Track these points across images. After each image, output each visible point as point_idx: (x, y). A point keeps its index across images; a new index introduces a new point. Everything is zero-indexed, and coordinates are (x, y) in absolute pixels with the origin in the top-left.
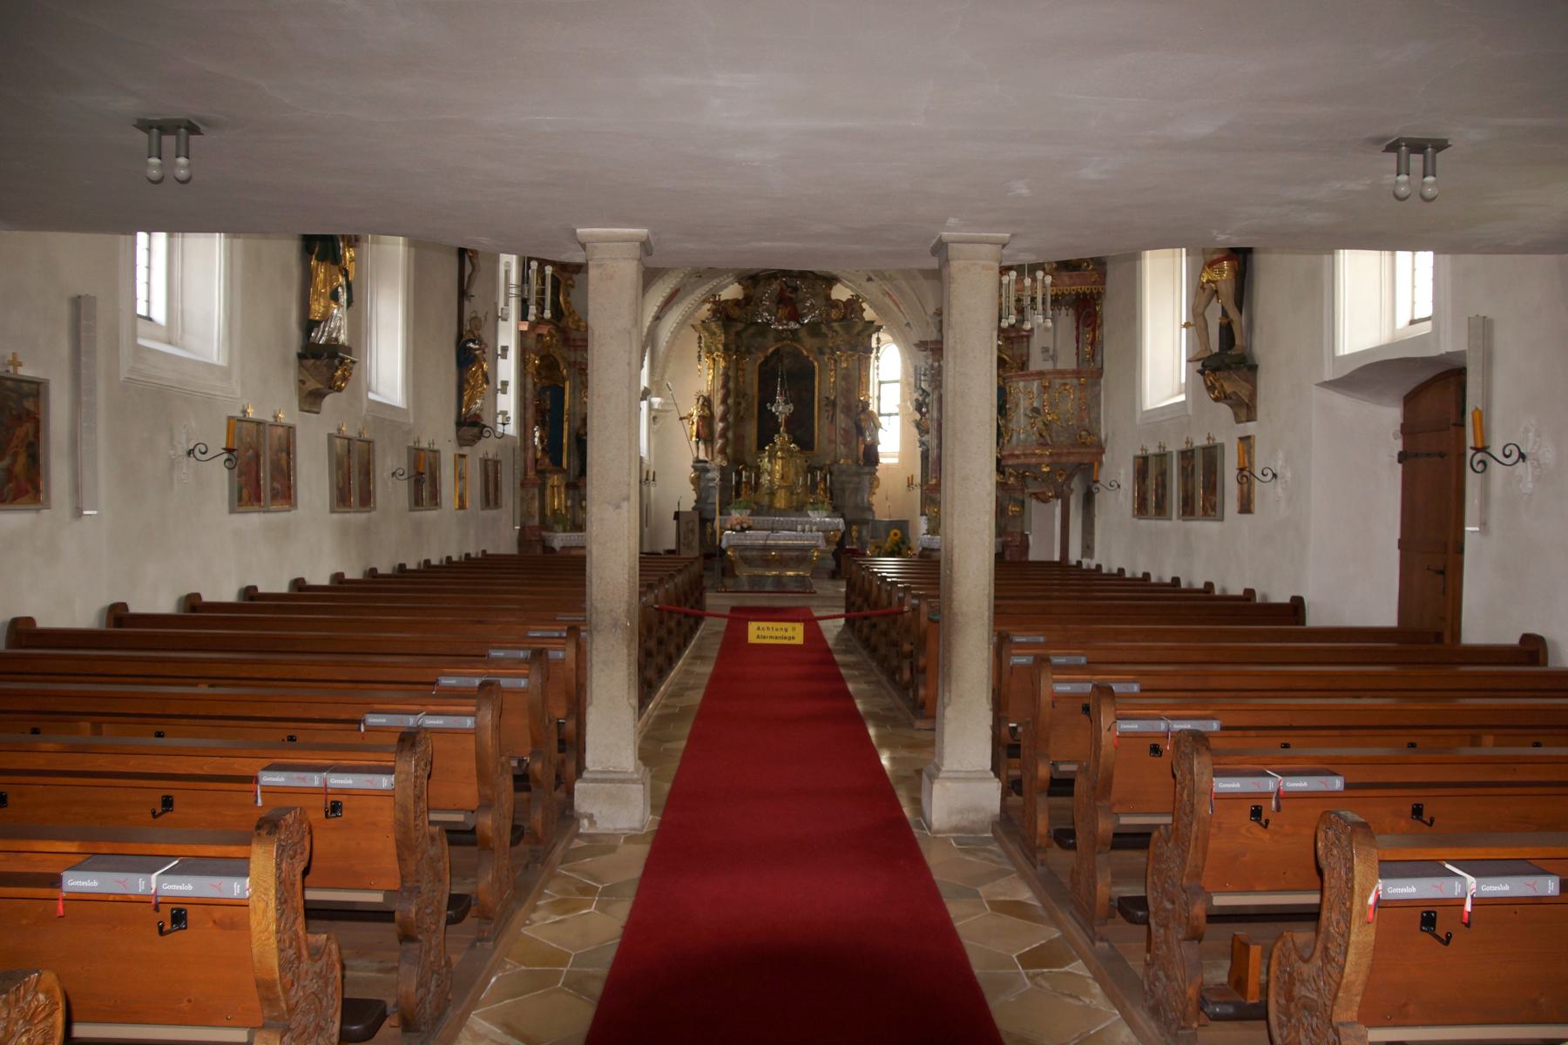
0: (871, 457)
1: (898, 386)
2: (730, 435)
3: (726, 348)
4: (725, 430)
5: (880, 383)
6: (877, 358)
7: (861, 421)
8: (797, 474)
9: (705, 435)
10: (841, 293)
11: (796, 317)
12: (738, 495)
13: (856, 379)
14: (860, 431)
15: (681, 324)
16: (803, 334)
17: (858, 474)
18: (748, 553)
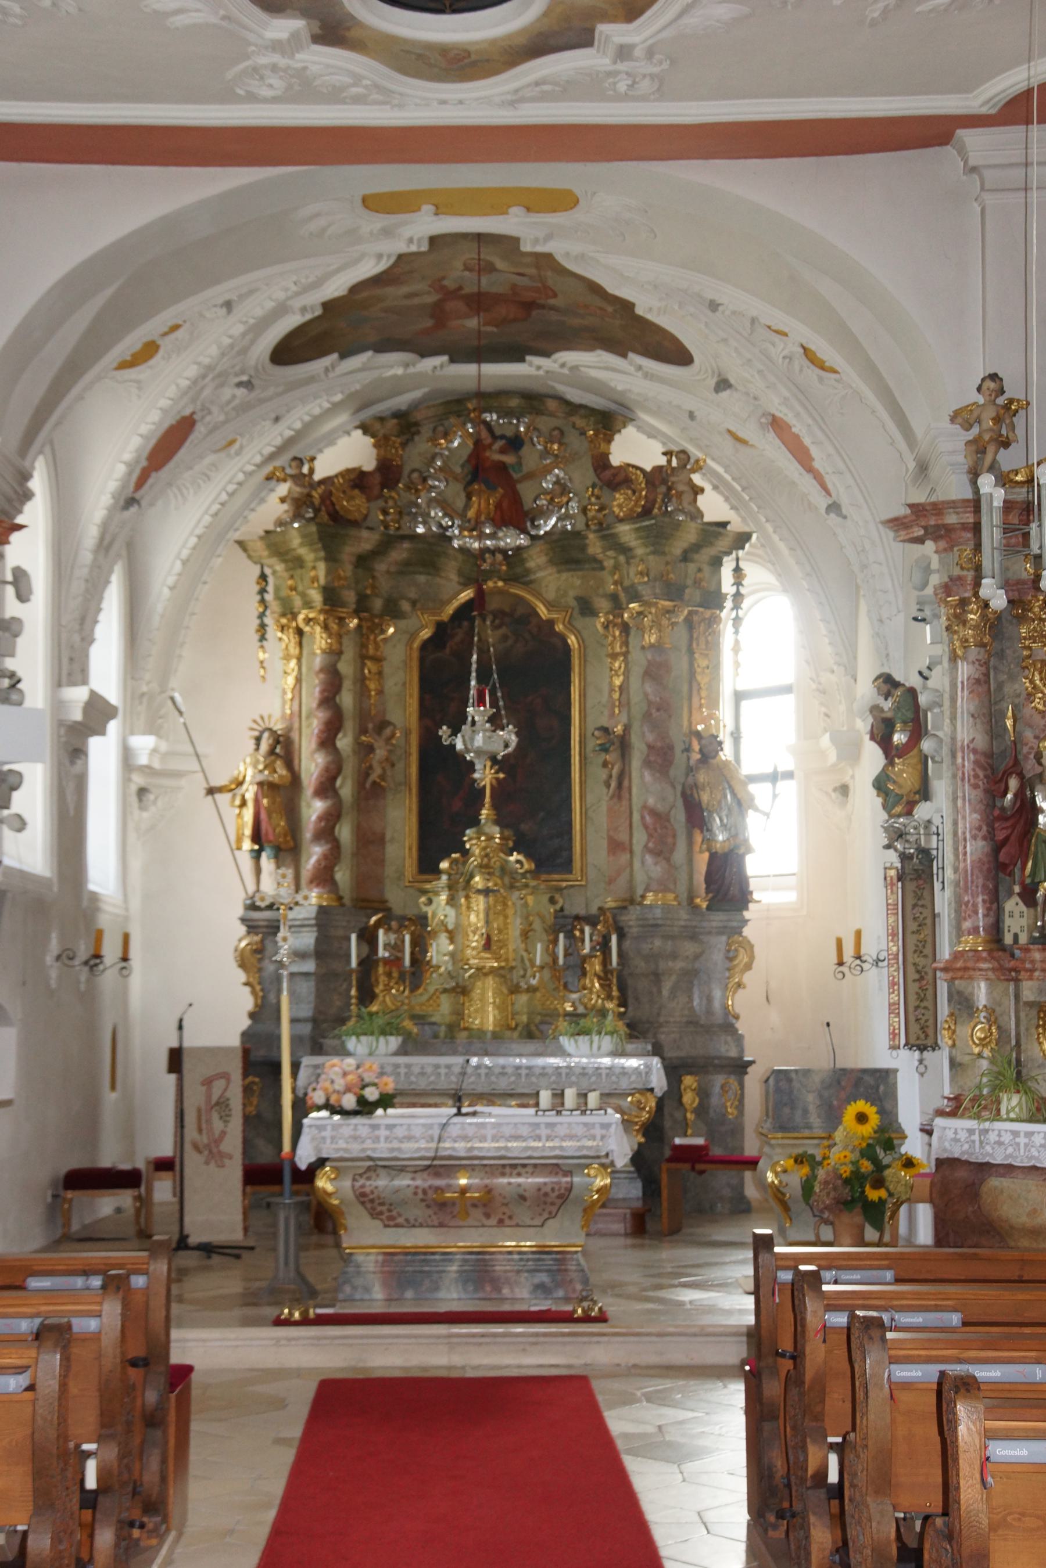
0: (726, 888)
2: (345, 832)
3: (331, 597)
5: (739, 697)
6: (737, 621)
7: (694, 790)
8: (525, 935)
9: (275, 835)
10: (635, 449)
11: (515, 515)
12: (367, 995)
13: (676, 683)
14: (696, 816)
15: (209, 542)
16: (537, 560)
17: (693, 936)
18: (381, 1183)
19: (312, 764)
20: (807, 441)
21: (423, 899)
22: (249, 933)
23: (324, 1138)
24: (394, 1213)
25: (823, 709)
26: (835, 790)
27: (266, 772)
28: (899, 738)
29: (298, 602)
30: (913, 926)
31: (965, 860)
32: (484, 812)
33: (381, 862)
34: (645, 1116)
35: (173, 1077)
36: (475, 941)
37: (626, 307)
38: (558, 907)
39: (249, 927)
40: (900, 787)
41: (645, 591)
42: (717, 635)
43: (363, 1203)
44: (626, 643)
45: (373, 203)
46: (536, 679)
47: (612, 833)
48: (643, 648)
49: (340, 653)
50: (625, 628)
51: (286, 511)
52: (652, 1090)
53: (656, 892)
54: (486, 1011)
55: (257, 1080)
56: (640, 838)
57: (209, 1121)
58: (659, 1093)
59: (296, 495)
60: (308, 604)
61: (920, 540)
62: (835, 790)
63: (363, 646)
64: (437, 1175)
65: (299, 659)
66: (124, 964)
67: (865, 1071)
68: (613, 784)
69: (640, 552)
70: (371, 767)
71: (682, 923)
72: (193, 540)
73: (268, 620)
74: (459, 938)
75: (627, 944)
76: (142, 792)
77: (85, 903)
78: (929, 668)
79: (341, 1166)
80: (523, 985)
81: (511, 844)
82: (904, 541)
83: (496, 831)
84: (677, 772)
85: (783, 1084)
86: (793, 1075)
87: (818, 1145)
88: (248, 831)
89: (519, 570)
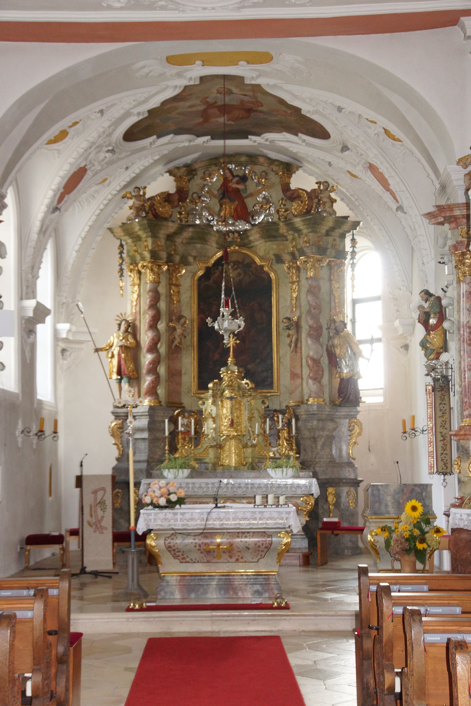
1: (379, 304)
2: (162, 370)
3: (154, 256)
4: (155, 363)
5: (354, 302)
6: (353, 265)
8: (250, 419)
9: (129, 372)
10: (303, 181)
11: (244, 214)
12: (173, 449)
16: (254, 236)
18: (178, 541)
19: (146, 337)
20: (387, 176)
21: (200, 402)
22: (116, 419)
23: (150, 520)
24: (185, 556)
25: (396, 308)
26: (402, 347)
27: (124, 341)
28: (432, 321)
29: (138, 257)
30: (439, 414)
31: (465, 381)
32: (230, 359)
33: (180, 384)
34: (309, 507)
35: (78, 490)
36: (226, 422)
37: (298, 110)
38: (266, 405)
39: (116, 416)
40: (433, 345)
41: (308, 251)
42: (343, 272)
43: (170, 551)
44: (298, 276)
45: (172, 60)
46: (254, 294)
47: (292, 369)
48: (307, 278)
49: (159, 283)
50: (298, 269)
51: (132, 213)
52: (312, 495)
53: (314, 398)
54: (231, 457)
55: (120, 491)
56: (306, 372)
57: (96, 511)
58: (316, 496)
59: (137, 206)
60: (143, 259)
61: (442, 224)
62: (402, 347)
63: (170, 279)
64: (206, 537)
65: (139, 285)
66: (55, 435)
67: (416, 485)
68: (293, 345)
69: (305, 231)
70: (174, 338)
71: (327, 413)
72: (87, 228)
73: (124, 267)
74: (218, 421)
75: (300, 423)
76: (63, 351)
77: (35, 406)
78: (447, 287)
79: (159, 533)
80: (249, 444)
81: (243, 375)
82: (433, 224)
83: (235, 369)
84: (324, 339)
85: (375, 492)
86: (380, 488)
87: (393, 522)
88: (115, 370)
89: (246, 241)
